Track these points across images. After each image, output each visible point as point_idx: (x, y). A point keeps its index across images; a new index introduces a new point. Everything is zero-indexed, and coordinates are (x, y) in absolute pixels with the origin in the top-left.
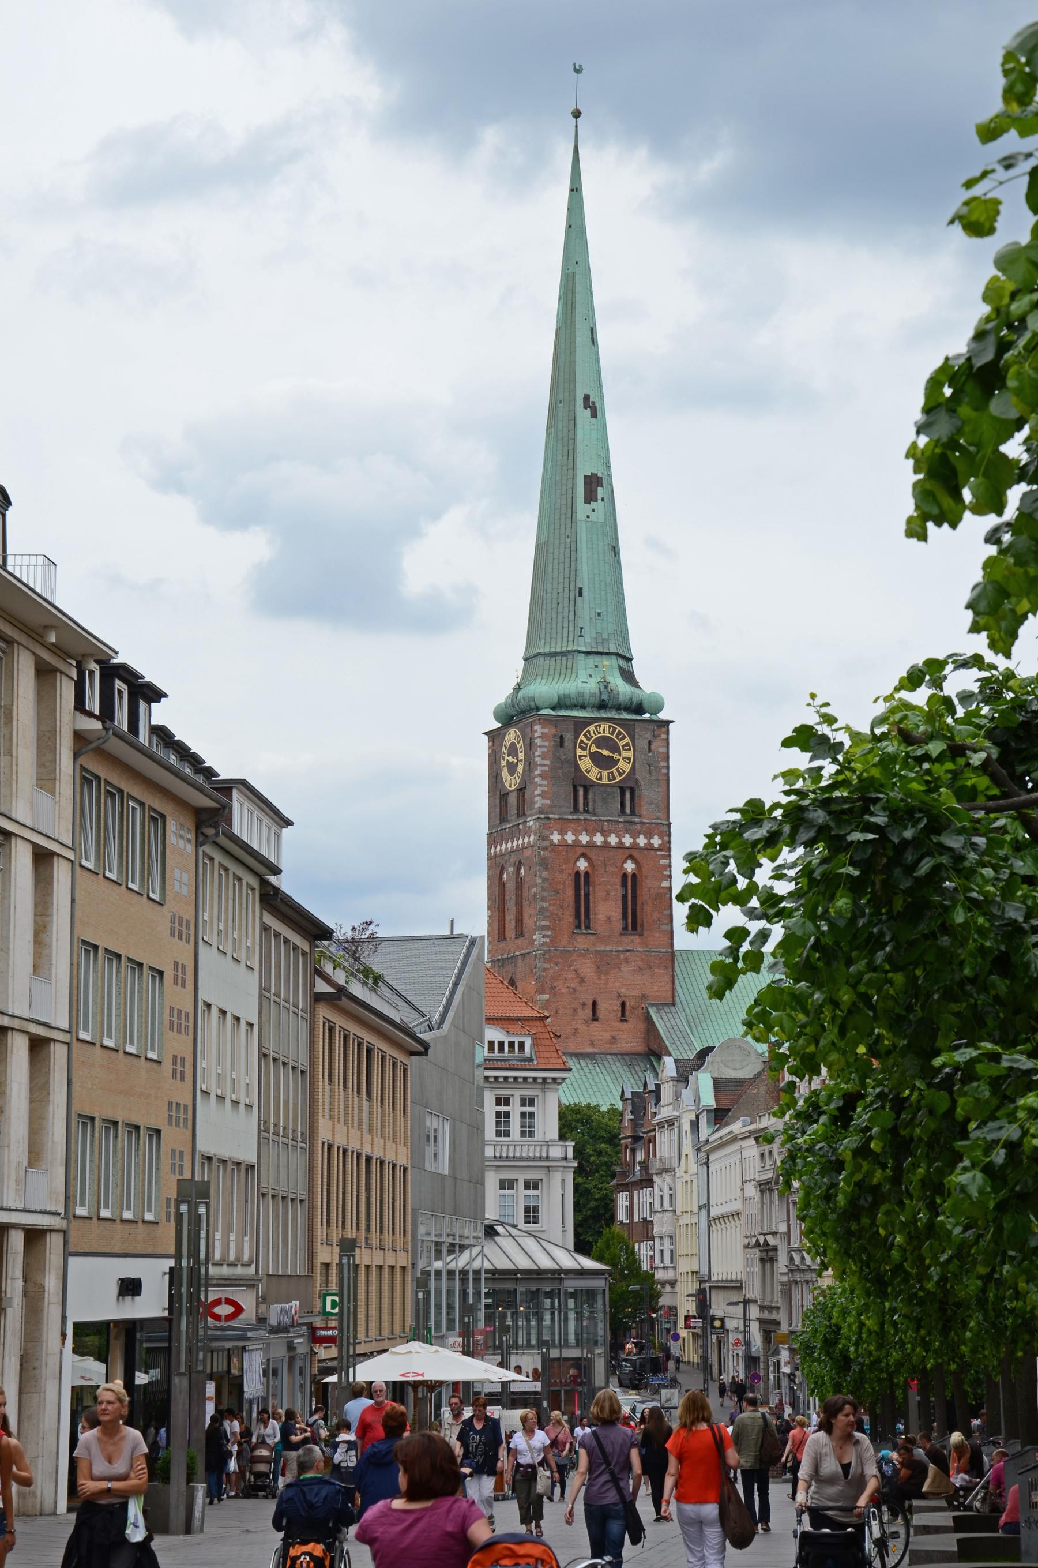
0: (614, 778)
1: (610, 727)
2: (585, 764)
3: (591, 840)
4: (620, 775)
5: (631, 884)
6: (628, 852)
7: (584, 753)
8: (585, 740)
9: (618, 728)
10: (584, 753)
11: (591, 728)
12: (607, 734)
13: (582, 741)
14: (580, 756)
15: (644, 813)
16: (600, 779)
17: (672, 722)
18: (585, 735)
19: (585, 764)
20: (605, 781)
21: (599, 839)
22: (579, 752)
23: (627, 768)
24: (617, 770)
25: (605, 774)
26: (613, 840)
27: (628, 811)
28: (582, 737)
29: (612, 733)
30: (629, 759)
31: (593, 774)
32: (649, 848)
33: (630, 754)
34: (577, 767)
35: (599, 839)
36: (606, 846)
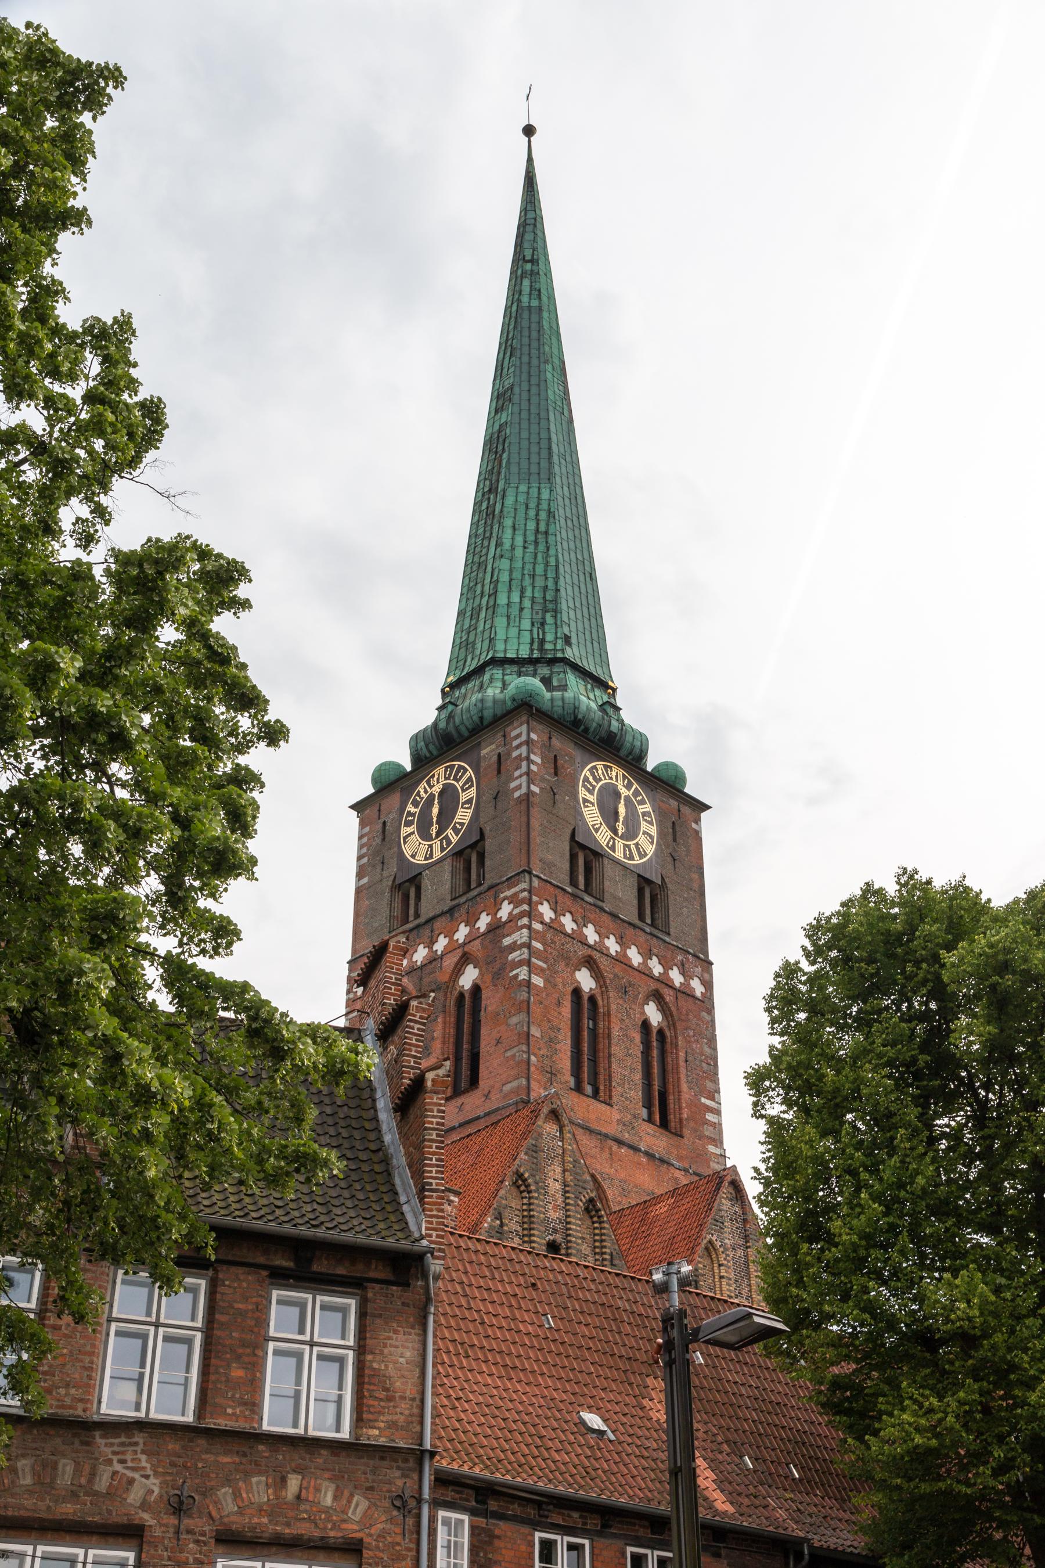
0: (632, 858)
1: (624, 777)
2: (592, 815)
3: (602, 942)
4: (641, 856)
5: (657, 1045)
6: (653, 985)
9: (635, 785)
11: (600, 765)
13: (586, 779)
14: (585, 801)
15: (672, 931)
17: (708, 807)
19: (592, 815)
20: (619, 855)
21: (612, 945)
24: (637, 845)
26: (634, 956)
27: (649, 921)
28: (586, 772)
31: (603, 837)
32: (685, 992)
33: (653, 830)
35: (612, 945)
36: (622, 960)
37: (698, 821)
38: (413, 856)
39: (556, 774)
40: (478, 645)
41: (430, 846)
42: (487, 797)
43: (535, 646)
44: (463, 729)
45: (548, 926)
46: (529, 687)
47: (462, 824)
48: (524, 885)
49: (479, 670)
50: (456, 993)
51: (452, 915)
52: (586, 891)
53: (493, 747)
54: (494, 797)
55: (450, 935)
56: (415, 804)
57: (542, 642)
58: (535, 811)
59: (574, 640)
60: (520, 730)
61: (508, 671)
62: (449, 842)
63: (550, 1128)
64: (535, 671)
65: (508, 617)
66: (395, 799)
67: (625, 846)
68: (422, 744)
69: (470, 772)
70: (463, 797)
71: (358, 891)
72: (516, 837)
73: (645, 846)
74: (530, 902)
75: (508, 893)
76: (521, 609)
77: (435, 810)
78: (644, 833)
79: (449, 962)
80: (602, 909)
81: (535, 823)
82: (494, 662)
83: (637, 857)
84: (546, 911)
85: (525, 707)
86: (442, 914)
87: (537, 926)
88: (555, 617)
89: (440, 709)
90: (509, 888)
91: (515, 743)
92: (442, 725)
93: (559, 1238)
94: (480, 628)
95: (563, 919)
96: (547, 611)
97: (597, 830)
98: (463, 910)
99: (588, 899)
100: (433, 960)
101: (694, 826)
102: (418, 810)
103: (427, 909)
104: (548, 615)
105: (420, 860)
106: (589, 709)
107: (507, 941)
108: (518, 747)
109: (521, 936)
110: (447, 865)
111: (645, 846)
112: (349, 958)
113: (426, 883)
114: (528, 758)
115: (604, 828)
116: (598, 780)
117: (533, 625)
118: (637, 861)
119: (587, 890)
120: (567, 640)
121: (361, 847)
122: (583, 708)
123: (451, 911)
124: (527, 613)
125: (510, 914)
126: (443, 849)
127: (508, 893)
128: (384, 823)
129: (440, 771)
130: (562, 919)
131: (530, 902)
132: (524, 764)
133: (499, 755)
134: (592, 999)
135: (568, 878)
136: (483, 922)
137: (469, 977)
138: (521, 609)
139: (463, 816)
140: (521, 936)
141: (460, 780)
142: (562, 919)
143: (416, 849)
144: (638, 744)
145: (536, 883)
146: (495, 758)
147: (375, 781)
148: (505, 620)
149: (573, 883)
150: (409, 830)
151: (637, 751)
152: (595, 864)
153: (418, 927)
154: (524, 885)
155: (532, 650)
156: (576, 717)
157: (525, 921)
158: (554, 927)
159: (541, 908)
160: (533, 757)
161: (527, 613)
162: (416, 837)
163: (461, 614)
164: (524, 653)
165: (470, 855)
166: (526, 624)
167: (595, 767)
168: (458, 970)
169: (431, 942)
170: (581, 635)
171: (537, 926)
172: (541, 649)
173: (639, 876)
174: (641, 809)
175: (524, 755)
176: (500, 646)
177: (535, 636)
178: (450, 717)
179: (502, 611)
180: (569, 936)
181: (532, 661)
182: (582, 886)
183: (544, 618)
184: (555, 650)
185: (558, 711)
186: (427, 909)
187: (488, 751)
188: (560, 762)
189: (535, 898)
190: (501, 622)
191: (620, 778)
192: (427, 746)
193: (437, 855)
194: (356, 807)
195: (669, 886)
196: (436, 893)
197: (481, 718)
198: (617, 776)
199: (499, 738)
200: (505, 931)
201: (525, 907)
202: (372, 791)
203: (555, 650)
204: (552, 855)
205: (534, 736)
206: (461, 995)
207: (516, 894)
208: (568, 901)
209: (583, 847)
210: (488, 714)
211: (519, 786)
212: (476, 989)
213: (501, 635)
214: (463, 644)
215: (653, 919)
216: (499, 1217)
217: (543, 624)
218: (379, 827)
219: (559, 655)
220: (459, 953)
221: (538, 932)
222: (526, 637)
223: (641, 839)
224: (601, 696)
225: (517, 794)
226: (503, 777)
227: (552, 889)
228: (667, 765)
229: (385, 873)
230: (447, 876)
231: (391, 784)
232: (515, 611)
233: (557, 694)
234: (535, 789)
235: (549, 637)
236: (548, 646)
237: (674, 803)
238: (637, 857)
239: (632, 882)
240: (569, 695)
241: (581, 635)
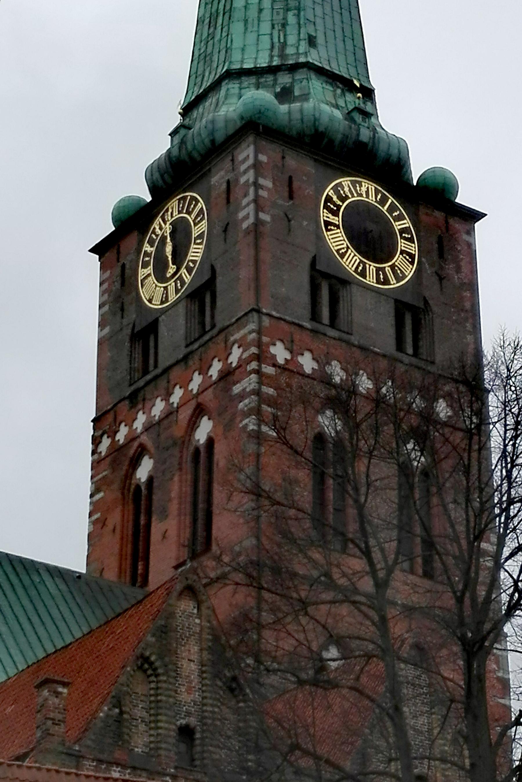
0: (386, 282)
1: (377, 192)
2: (337, 240)
4: (398, 280)
7: (332, 219)
8: (335, 198)
9: (391, 200)
10: (332, 219)
11: (346, 182)
12: (372, 199)
13: (329, 199)
14: (327, 224)
16: (363, 274)
18: (335, 189)
20: (371, 280)
22: (324, 215)
23: (410, 272)
24: (393, 267)
25: (372, 267)
27: (410, 351)
28: (329, 191)
29: (383, 201)
30: (412, 256)
33: (414, 249)
34: (320, 239)
37: (471, 232)
38: (150, 301)
39: (291, 197)
40: (215, 58)
41: (166, 288)
42: (218, 230)
43: (276, 52)
44: (195, 155)
45: (282, 369)
46: (257, 103)
47: (194, 262)
48: (252, 326)
49: (216, 86)
50: (192, 449)
51: (186, 363)
52: (333, 324)
53: (222, 173)
54: (223, 229)
55: (185, 385)
56: (151, 243)
57: (284, 45)
58: (266, 243)
59: (320, 40)
60: (247, 153)
61: (245, 84)
62: (183, 283)
63: (187, 606)
64: (275, 80)
65: (246, 21)
66: (132, 239)
67: (378, 270)
68: (157, 175)
69: (202, 204)
70: (195, 232)
71: (100, 343)
72: (245, 273)
73: (404, 267)
74: (259, 344)
75: (237, 336)
76: (260, 11)
77: (169, 249)
78: (402, 252)
79: (185, 415)
80: (348, 343)
81: (266, 256)
82: (230, 75)
83: (393, 280)
84: (280, 353)
85: (254, 127)
86: (178, 362)
87: (269, 370)
88: (298, 16)
89: (173, 134)
90: (239, 329)
91: (243, 168)
92: (175, 152)
93: (193, 721)
94: (217, 37)
95: (301, 359)
96: (288, 10)
97: (342, 256)
98: (196, 357)
99: (332, 333)
100: (170, 413)
101: (465, 237)
102: (153, 249)
103: (165, 359)
104: (290, 14)
105: (156, 305)
106: (332, 118)
107: (237, 389)
108: (245, 172)
109: (250, 382)
110: (181, 309)
111: (404, 267)
112: (94, 416)
113: (163, 330)
114: (256, 184)
115: (352, 252)
116: (343, 199)
117: (273, 27)
118: (394, 284)
119: (333, 324)
120: (312, 41)
121: (102, 294)
122: (324, 120)
123: (185, 358)
124: (266, 14)
125: (240, 359)
126: (177, 291)
127: (237, 336)
128: (123, 266)
129: (173, 205)
130: (300, 359)
131: (259, 344)
132: (252, 190)
133: (228, 182)
134: (338, 443)
135: (307, 313)
136: (215, 369)
137: (204, 430)
138: (260, 11)
139: (196, 252)
140: (250, 382)
141: (192, 210)
142: (300, 359)
143: (153, 292)
144: (394, 152)
145: (266, 322)
146: (224, 186)
147: (115, 220)
148: (241, 25)
149: (315, 316)
150: (146, 271)
151: (394, 159)
152: (343, 293)
153: (156, 378)
154: (252, 326)
155: (271, 57)
156: (316, 130)
157: (254, 365)
158: (290, 369)
159: (273, 350)
160: (261, 181)
161: (266, 14)
162: (152, 279)
163: (200, 21)
164: (263, 62)
165: (202, 295)
166: (266, 27)
167: (340, 184)
168: (193, 424)
169: (169, 394)
170: (330, 34)
171: (269, 370)
172: (282, 55)
173: (396, 301)
174: (397, 226)
175: (251, 180)
176: (236, 56)
177: (276, 40)
178: (183, 142)
179: (238, 15)
180: (308, 376)
181: (272, 70)
182: (326, 320)
183: (285, 18)
184: (298, 54)
185: (297, 125)
186: (165, 359)
187: (218, 178)
188: (296, 184)
189: (265, 339)
190: (237, 28)
191: (372, 193)
192: (162, 176)
193: (173, 297)
194: (97, 249)
195: (435, 309)
196: (171, 339)
197: (213, 141)
198: (367, 191)
199: (227, 164)
200: (235, 378)
201: (254, 350)
202: (114, 229)
203: (298, 54)
204: (292, 288)
205: (263, 158)
206: (197, 450)
207: (244, 336)
208: (306, 337)
209: (326, 276)
210: (220, 137)
211: (246, 215)
212: (210, 442)
213: (237, 43)
214: (201, 57)
215: (416, 347)
216: (118, 703)
217: (284, 25)
218: (118, 270)
219: (302, 60)
220: (193, 404)
221: (268, 376)
222: (266, 42)
223: (398, 259)
224: (353, 100)
225: (245, 225)
226: (232, 208)
227: (286, 327)
228: (433, 171)
229: (125, 321)
230: (182, 321)
231: (132, 222)
232: (253, 13)
233: (297, 105)
234: (265, 217)
235: (292, 39)
236: (290, 51)
237: (439, 215)
238: (393, 280)
239: (387, 310)
240: (309, 106)
241: (330, 34)
